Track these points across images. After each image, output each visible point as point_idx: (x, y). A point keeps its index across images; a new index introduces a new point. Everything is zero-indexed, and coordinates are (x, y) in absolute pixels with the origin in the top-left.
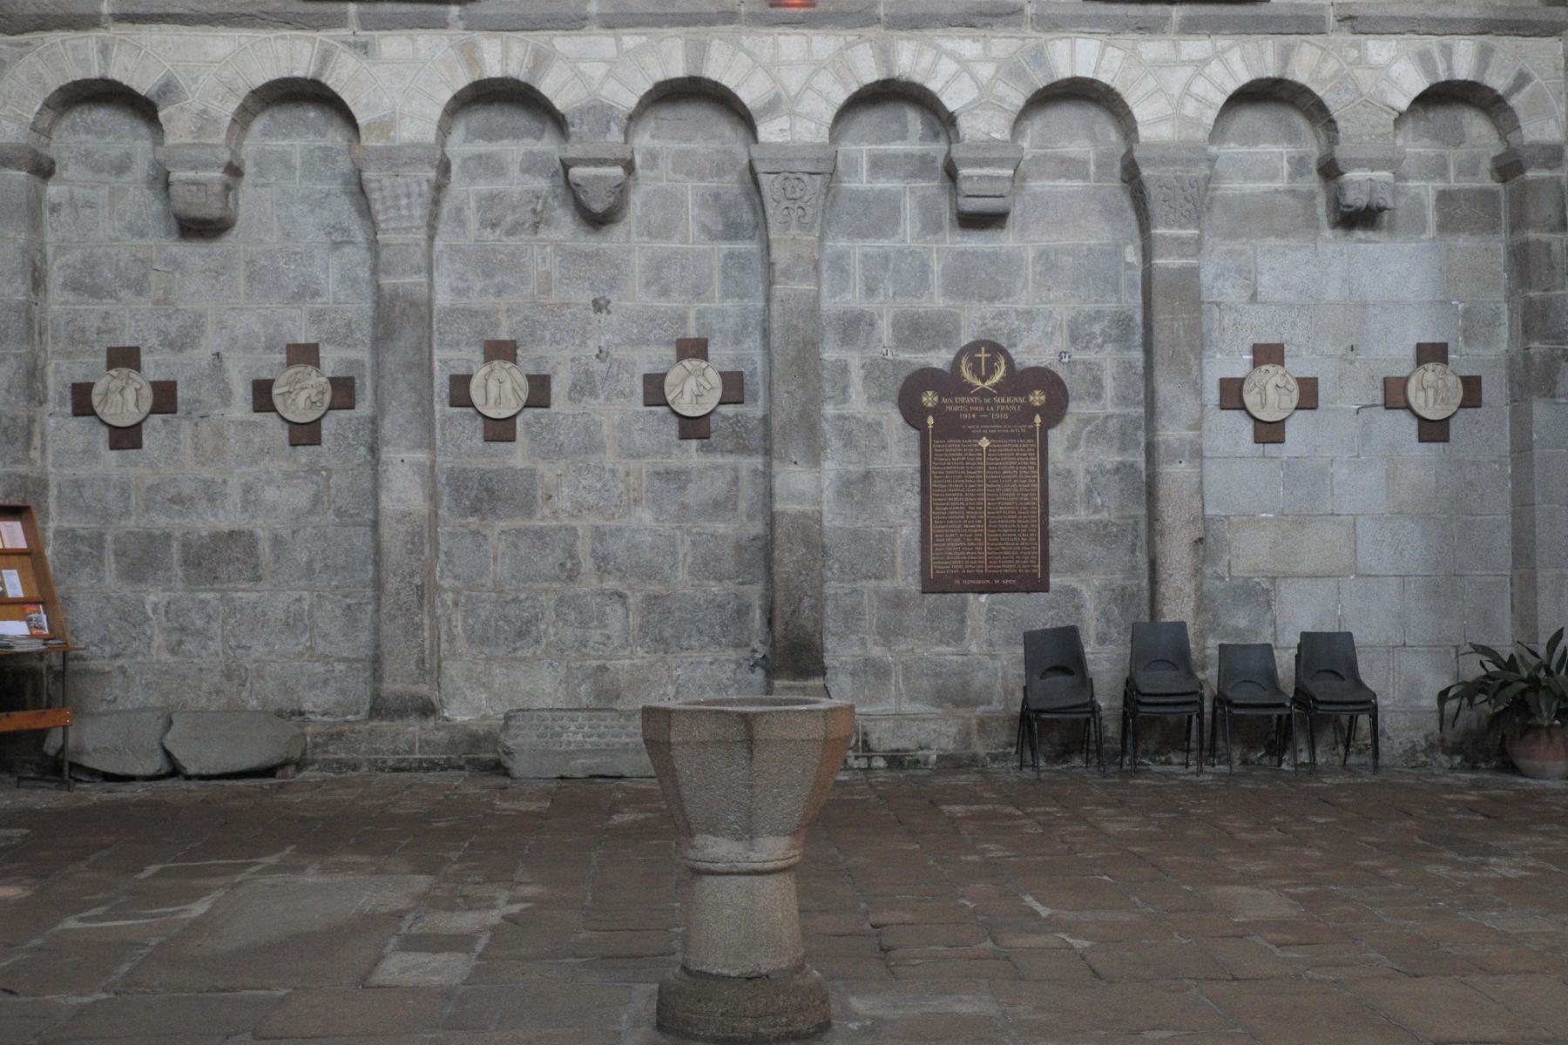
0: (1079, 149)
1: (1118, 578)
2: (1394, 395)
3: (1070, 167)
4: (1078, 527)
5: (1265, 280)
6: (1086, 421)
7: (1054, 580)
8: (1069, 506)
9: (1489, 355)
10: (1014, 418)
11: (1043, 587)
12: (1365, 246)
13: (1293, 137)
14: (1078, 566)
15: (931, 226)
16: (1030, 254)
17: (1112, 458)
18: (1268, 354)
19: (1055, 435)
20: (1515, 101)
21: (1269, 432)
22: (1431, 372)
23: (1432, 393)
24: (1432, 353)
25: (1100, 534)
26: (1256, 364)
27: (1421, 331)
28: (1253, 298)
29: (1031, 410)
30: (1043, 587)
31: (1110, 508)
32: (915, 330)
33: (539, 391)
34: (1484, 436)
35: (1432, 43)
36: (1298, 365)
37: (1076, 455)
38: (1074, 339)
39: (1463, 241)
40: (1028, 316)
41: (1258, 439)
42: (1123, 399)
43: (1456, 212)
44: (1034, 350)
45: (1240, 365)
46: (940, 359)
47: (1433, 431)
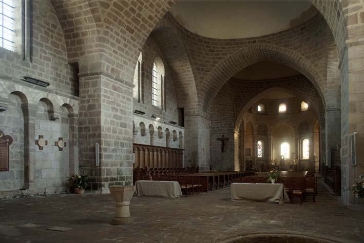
0: (15, 101)
1: (20, 169)
2: (56, 144)
3: (13, 104)
4: (14, 161)
5: (41, 126)
6: (14, 145)
7: (10, 169)
8: (12, 158)
9: (67, 139)
10: (4, 143)
11: (8, 170)
12: (53, 124)
13: (45, 106)
14: (13, 167)
16: (7, 117)
17: (19, 151)
18: (40, 137)
19: (10, 146)
20: (73, 108)
21: (41, 148)
22: (61, 141)
23: (61, 144)
24: (60, 139)
25: (17, 162)
26: (39, 138)
27: (59, 136)
28: (39, 128)
29: (6, 142)
30: (8, 170)
31: (20, 158)
34: (66, 150)
35: (64, 98)
36: (45, 139)
38: (13, 131)
39: (64, 124)
40: (6, 127)
41: (39, 149)
42: (20, 142)
43: (64, 120)
44: (7, 132)
45: (37, 138)
47: (61, 149)
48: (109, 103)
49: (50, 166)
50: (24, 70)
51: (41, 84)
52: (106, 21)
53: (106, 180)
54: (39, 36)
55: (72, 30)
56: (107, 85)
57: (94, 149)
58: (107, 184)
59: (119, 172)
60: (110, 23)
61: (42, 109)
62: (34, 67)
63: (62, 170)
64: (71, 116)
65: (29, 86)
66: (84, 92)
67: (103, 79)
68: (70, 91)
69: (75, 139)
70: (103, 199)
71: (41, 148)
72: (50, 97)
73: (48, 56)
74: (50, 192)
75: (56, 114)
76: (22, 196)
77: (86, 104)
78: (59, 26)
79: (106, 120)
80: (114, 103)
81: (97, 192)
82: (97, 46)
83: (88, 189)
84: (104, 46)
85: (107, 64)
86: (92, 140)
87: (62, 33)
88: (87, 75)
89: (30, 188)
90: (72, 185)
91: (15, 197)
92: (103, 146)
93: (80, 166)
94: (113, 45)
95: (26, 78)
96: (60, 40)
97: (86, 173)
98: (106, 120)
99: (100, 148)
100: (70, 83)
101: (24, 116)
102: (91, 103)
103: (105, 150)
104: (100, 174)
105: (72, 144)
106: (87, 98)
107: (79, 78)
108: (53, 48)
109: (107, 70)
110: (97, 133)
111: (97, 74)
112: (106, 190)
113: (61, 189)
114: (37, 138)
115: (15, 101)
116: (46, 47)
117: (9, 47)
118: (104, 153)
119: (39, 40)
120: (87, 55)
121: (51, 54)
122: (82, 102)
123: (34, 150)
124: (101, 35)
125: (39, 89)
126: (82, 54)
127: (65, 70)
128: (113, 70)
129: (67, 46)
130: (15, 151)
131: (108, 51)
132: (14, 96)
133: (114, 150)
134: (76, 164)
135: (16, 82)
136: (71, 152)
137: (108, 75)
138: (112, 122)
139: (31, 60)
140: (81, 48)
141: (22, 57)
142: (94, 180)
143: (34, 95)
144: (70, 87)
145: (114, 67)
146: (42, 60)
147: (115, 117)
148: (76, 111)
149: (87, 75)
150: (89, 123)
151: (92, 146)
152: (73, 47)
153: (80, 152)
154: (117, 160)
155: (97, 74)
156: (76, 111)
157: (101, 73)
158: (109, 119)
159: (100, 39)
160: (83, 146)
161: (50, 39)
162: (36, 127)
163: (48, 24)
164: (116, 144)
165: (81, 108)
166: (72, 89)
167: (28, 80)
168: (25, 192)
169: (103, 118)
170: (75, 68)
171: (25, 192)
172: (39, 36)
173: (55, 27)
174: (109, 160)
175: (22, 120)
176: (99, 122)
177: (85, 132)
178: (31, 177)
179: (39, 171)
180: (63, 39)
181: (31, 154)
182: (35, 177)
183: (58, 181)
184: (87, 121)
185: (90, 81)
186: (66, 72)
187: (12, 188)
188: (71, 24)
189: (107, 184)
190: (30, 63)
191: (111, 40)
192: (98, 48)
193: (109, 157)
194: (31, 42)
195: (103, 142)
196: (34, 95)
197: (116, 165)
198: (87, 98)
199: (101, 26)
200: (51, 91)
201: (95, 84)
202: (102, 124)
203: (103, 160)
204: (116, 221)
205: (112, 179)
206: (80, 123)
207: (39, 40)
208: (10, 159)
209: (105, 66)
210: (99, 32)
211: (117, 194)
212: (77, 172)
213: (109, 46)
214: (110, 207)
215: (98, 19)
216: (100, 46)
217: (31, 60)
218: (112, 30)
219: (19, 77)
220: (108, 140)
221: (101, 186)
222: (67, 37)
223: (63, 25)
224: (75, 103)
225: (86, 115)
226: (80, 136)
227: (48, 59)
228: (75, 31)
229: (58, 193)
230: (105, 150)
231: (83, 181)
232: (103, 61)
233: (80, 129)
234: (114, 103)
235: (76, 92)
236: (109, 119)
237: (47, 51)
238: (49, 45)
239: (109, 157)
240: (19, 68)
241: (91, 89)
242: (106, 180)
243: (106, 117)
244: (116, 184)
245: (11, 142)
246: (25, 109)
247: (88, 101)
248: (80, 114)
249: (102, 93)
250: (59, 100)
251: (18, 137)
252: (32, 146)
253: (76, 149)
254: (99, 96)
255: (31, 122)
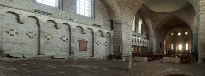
3: (88, 32)
9: (108, 43)
11: (86, 51)
15: (80, 33)
18: (98, 42)
19: (87, 44)
21: (98, 45)
23: (106, 44)
25: (89, 49)
30: (86, 51)
32: (79, 38)
33: (52, 37)
37: (89, 45)
39: (108, 39)
44: (86, 40)
45: (97, 42)
46: (81, 40)
47: (106, 46)
48: (125, 32)
49: (102, 50)
50: (92, 22)
51: (100, 26)
52: (124, 6)
53: (124, 56)
54: (97, 12)
55: (110, 10)
56: (124, 27)
57: (119, 47)
58: (124, 58)
59: (128, 54)
60: (125, 7)
61: (99, 33)
62: (96, 21)
63: (106, 52)
64: (110, 36)
65: (94, 27)
66: (116, 29)
67: (123, 25)
68: (110, 28)
69: (112, 43)
70: (122, 62)
71: (98, 45)
72: (102, 30)
73: (101, 18)
74: (101, 58)
75: (104, 35)
76: (91, 58)
77: (116, 33)
78: (105, 9)
79: (124, 38)
80: (126, 32)
81: (121, 60)
82: (120, 14)
83: (117, 59)
84: (123, 15)
85: (124, 20)
86: (119, 44)
87: (106, 11)
88: (117, 24)
89: (94, 57)
90: (110, 57)
91: (89, 58)
92: (123, 46)
93: (113, 52)
94: (126, 14)
95: (93, 24)
96: (106, 13)
97: (116, 54)
98: (124, 38)
99: (122, 47)
100: (110, 26)
101: (92, 35)
102: (118, 32)
103: (124, 47)
104: (122, 55)
105: (110, 44)
106: (117, 31)
107: (112, 25)
108: (103, 15)
109: (124, 22)
110: (121, 42)
111: (120, 23)
112: (124, 60)
113: (106, 58)
114: (97, 42)
115: (89, 31)
116: (100, 15)
117: (87, 15)
118: (123, 48)
119: (98, 13)
120: (116, 17)
121: (102, 17)
122: (114, 32)
123: (96, 46)
124: (123, 11)
125: (98, 28)
126: (115, 17)
127: (108, 22)
128: (126, 22)
129: (108, 15)
130: (89, 45)
131: (125, 16)
132: (89, 29)
133: (127, 47)
134: (112, 51)
135: (89, 25)
136: (110, 47)
137: (124, 24)
138: (126, 38)
139: (95, 19)
140: (114, 15)
141: (91, 18)
142: (119, 56)
143: (96, 29)
144: (109, 27)
145: (126, 21)
146: (99, 19)
147: (127, 37)
148: (112, 34)
149: (117, 24)
150: (118, 38)
151: (119, 45)
152: (111, 15)
153: (113, 47)
154: (127, 50)
155: (120, 23)
156: (112, 34)
157: (122, 23)
158: (125, 37)
159: (122, 12)
160: (114, 45)
161: (102, 13)
162: (97, 39)
163: (101, 8)
164: (127, 45)
165: (114, 34)
166: (110, 28)
167: (94, 25)
168: (92, 58)
169: (123, 37)
170: (112, 22)
171: (92, 58)
172: (97, 12)
173: (104, 9)
174: (125, 50)
175: (92, 36)
176: (122, 38)
177: (116, 41)
178: (95, 53)
179: (98, 52)
180: (107, 13)
181: (95, 47)
182: (96, 54)
183: (105, 55)
184: (117, 38)
185: (118, 26)
186: (108, 23)
187: (88, 56)
188: (110, 8)
189: (124, 58)
190: (94, 20)
191: (125, 13)
192: (121, 15)
193: (125, 49)
194: (95, 14)
195: (123, 45)
196: (96, 29)
197: (127, 52)
198: (117, 31)
199: (122, 8)
200: (102, 28)
201: (120, 26)
202: (123, 39)
203: (123, 50)
204: (127, 70)
205: (126, 56)
206: (114, 38)
207: (98, 13)
208: (87, 48)
209: (124, 21)
210: (121, 10)
211: (127, 61)
212: (112, 53)
213: (125, 14)
214: (125, 65)
215: (121, 6)
216: (122, 14)
217: (95, 19)
218: (126, 9)
219: (90, 24)
220: (125, 44)
221: (122, 58)
222: (108, 12)
223: (107, 8)
224: (112, 33)
225: (116, 36)
226: (114, 42)
227: (101, 19)
228: (111, 10)
229: (105, 59)
230: (124, 47)
231: (115, 56)
232: (123, 19)
233: (114, 40)
234: (126, 32)
235: (112, 28)
236: (125, 37)
237: (101, 16)
238: (101, 14)
239: (125, 49)
240: (91, 21)
241: (118, 28)
242: (124, 56)
243: (124, 37)
244: (127, 58)
245: (87, 42)
246: (93, 33)
247: (117, 32)
248: (114, 36)
249: (123, 29)
250: (105, 31)
251: (90, 42)
252: (95, 44)
253: (112, 46)
254: (122, 30)
255: (94, 37)
